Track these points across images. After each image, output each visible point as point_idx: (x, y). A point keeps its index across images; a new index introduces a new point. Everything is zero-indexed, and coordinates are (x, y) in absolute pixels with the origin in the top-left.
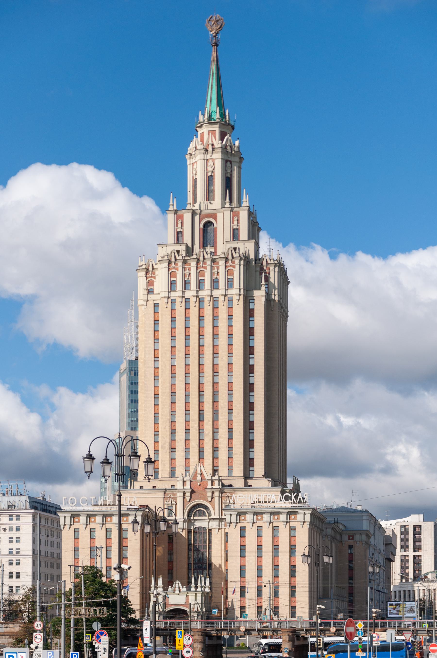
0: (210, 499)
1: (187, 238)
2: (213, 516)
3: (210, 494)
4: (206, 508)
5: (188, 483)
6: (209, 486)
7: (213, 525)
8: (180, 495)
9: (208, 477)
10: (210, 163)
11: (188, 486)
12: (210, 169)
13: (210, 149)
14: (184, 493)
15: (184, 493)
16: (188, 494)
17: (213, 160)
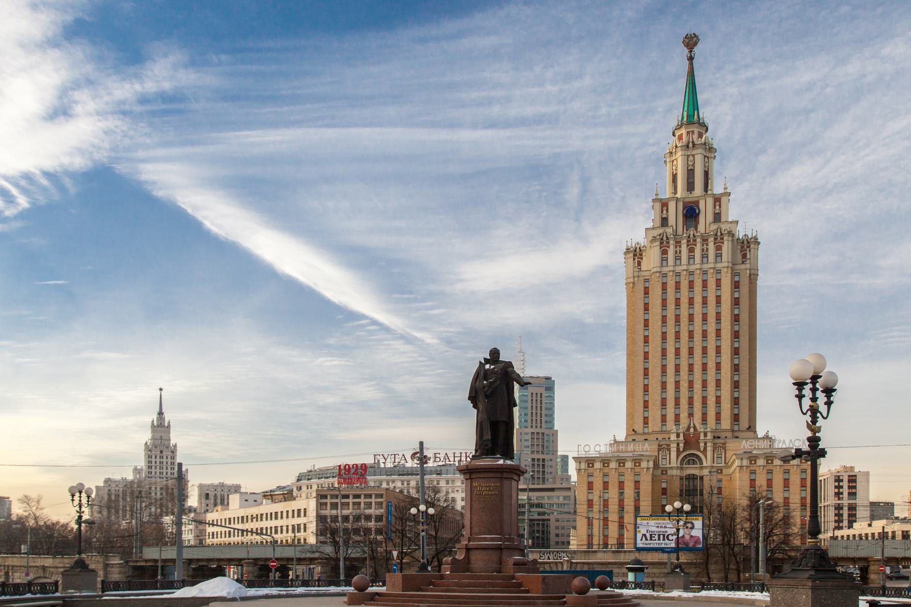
0: (702, 449)
1: (672, 221)
2: (705, 464)
3: (702, 445)
4: (697, 456)
5: (681, 435)
6: (702, 437)
7: (705, 472)
8: (673, 447)
9: (700, 428)
10: (691, 158)
11: (682, 438)
12: (690, 163)
13: (691, 145)
14: (678, 445)
15: (678, 445)
16: (681, 445)
17: (693, 156)
